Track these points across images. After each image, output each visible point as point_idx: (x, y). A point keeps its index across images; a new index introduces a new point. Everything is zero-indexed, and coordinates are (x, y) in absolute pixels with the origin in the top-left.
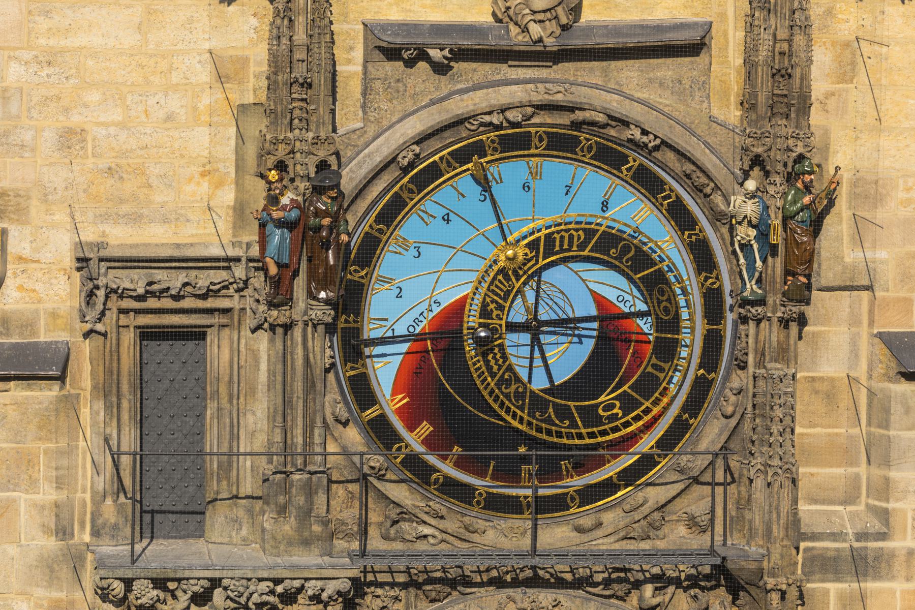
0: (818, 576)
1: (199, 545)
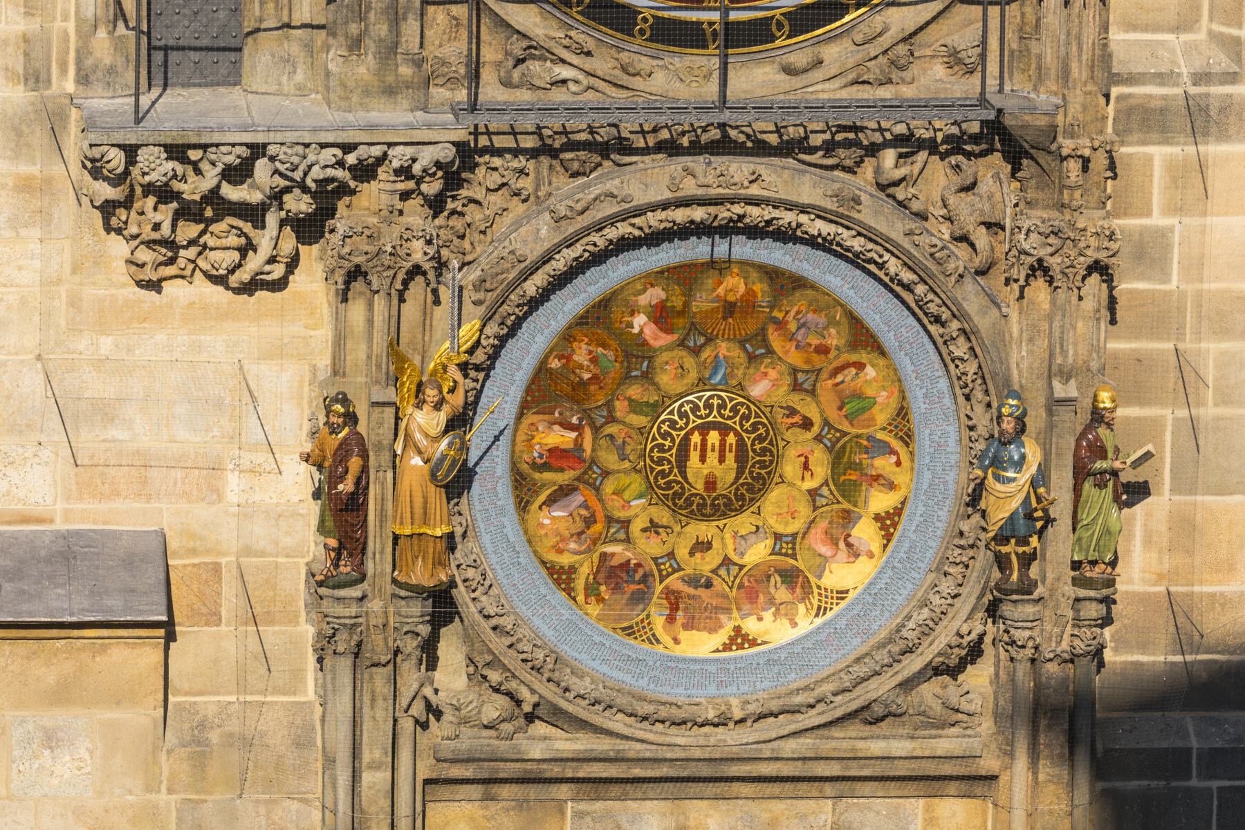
0: (1136, 136)
1: (234, 95)
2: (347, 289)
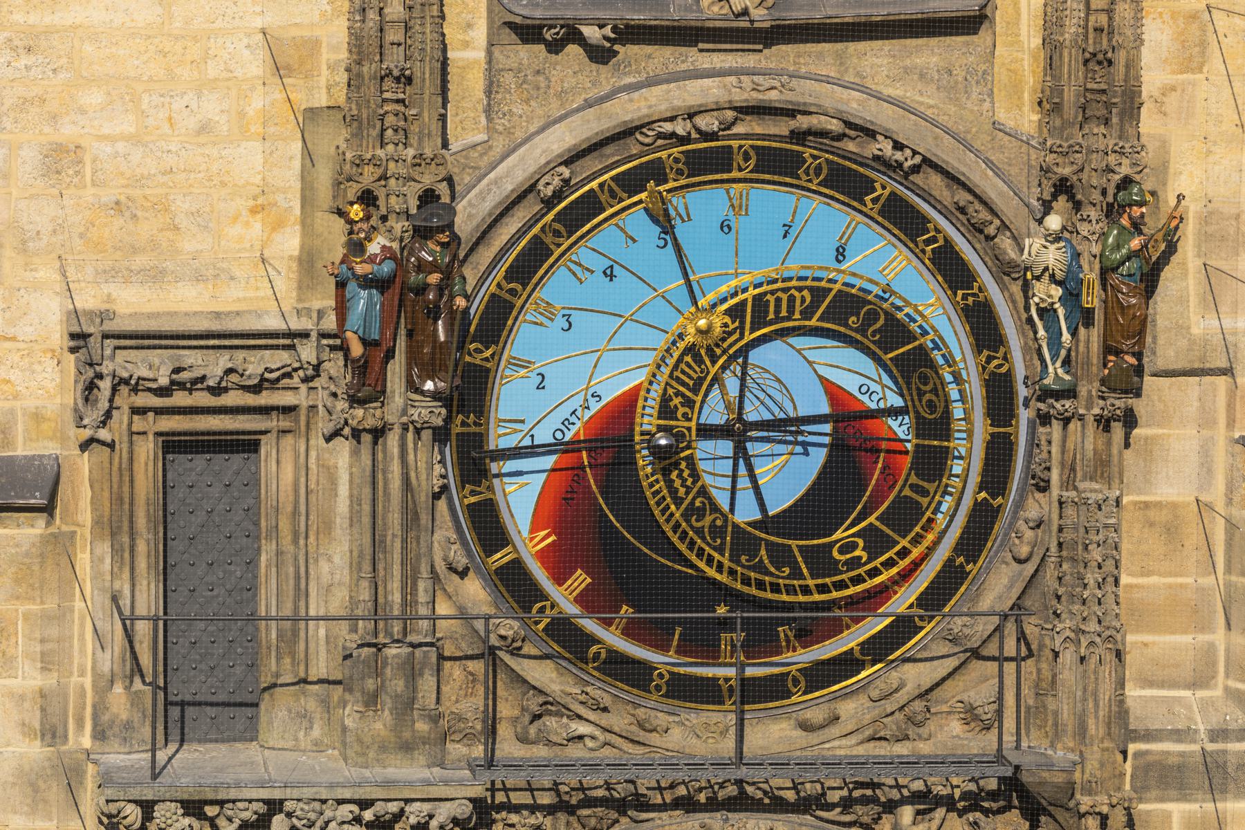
0: (1154, 793)
1: (251, 751)
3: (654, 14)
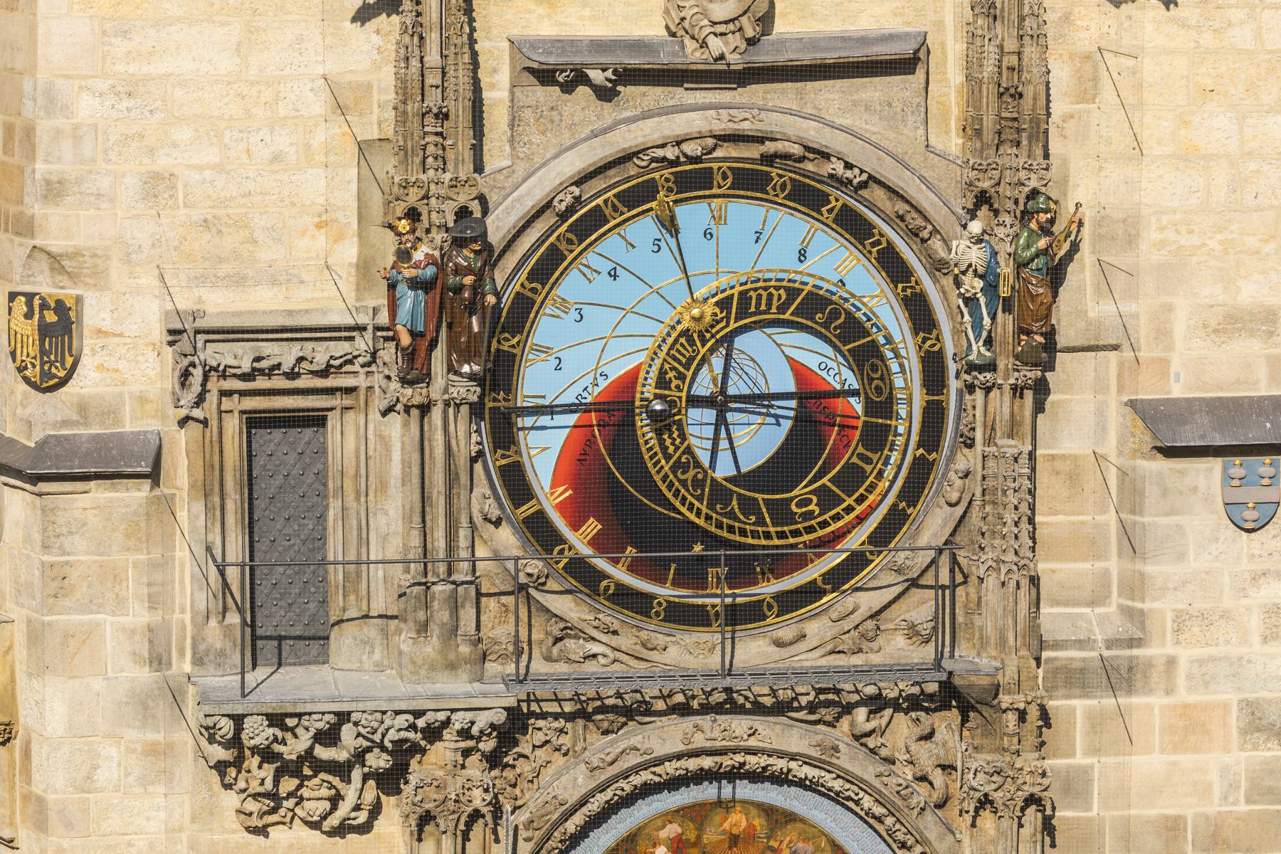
0: (1062, 692)
1: (321, 673)
2: (420, 831)
3: (647, 59)
